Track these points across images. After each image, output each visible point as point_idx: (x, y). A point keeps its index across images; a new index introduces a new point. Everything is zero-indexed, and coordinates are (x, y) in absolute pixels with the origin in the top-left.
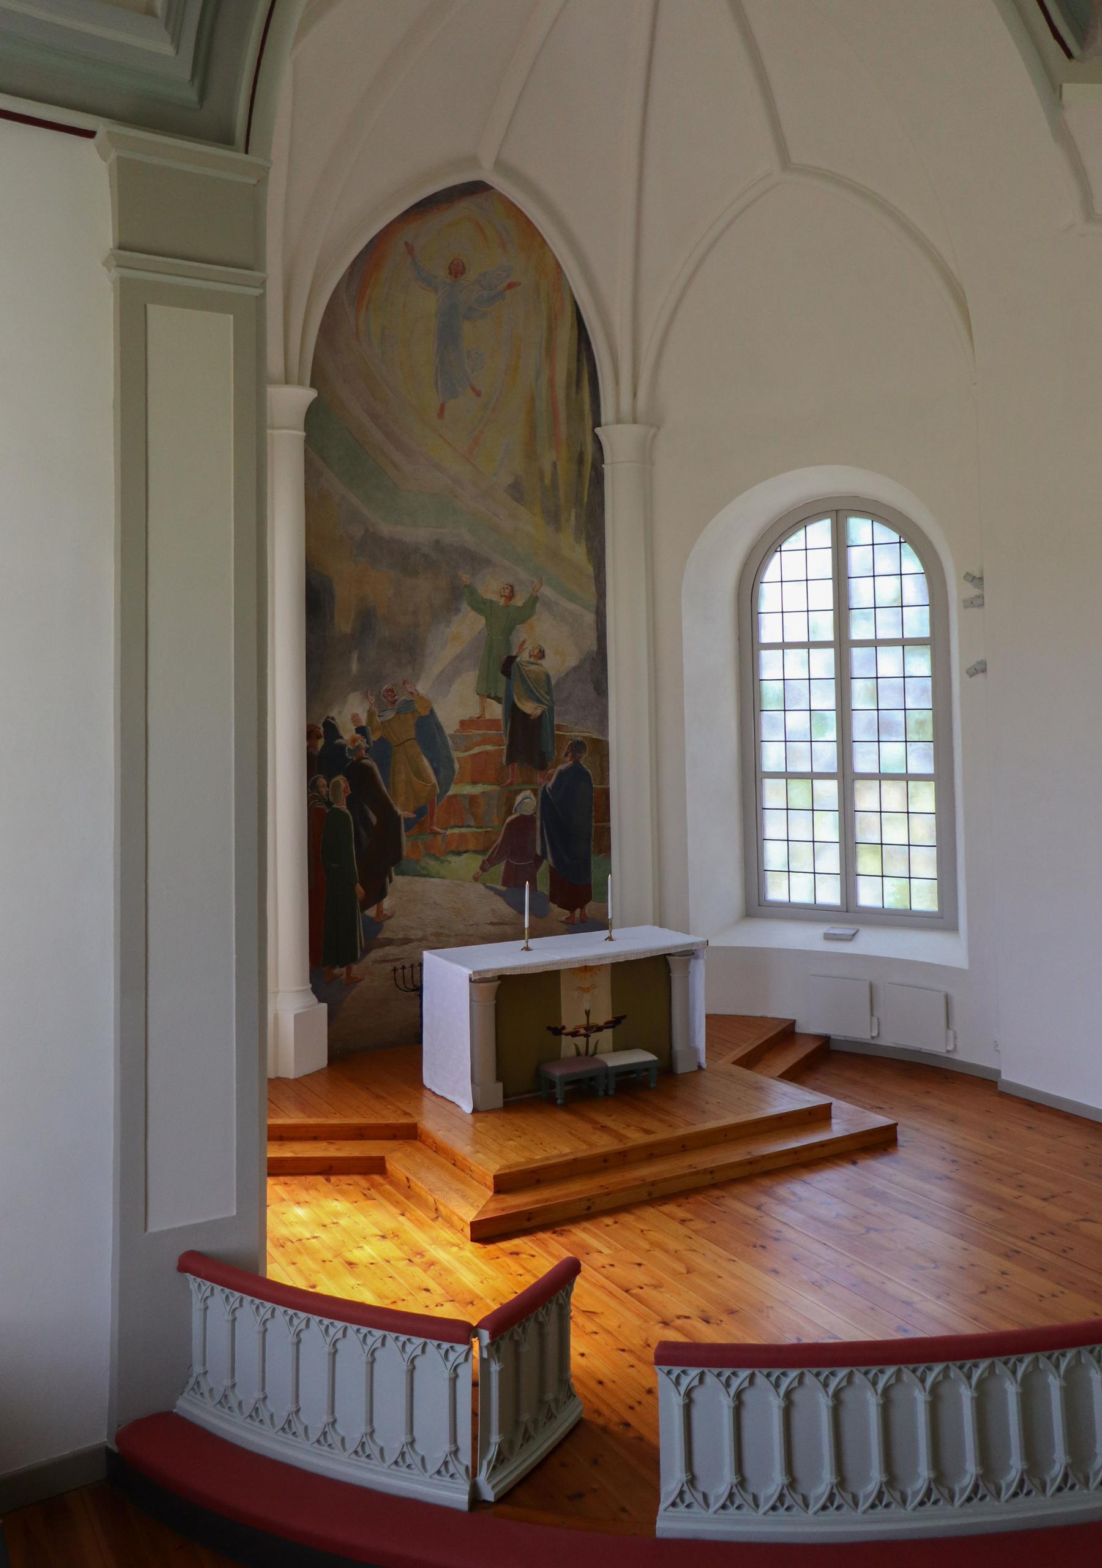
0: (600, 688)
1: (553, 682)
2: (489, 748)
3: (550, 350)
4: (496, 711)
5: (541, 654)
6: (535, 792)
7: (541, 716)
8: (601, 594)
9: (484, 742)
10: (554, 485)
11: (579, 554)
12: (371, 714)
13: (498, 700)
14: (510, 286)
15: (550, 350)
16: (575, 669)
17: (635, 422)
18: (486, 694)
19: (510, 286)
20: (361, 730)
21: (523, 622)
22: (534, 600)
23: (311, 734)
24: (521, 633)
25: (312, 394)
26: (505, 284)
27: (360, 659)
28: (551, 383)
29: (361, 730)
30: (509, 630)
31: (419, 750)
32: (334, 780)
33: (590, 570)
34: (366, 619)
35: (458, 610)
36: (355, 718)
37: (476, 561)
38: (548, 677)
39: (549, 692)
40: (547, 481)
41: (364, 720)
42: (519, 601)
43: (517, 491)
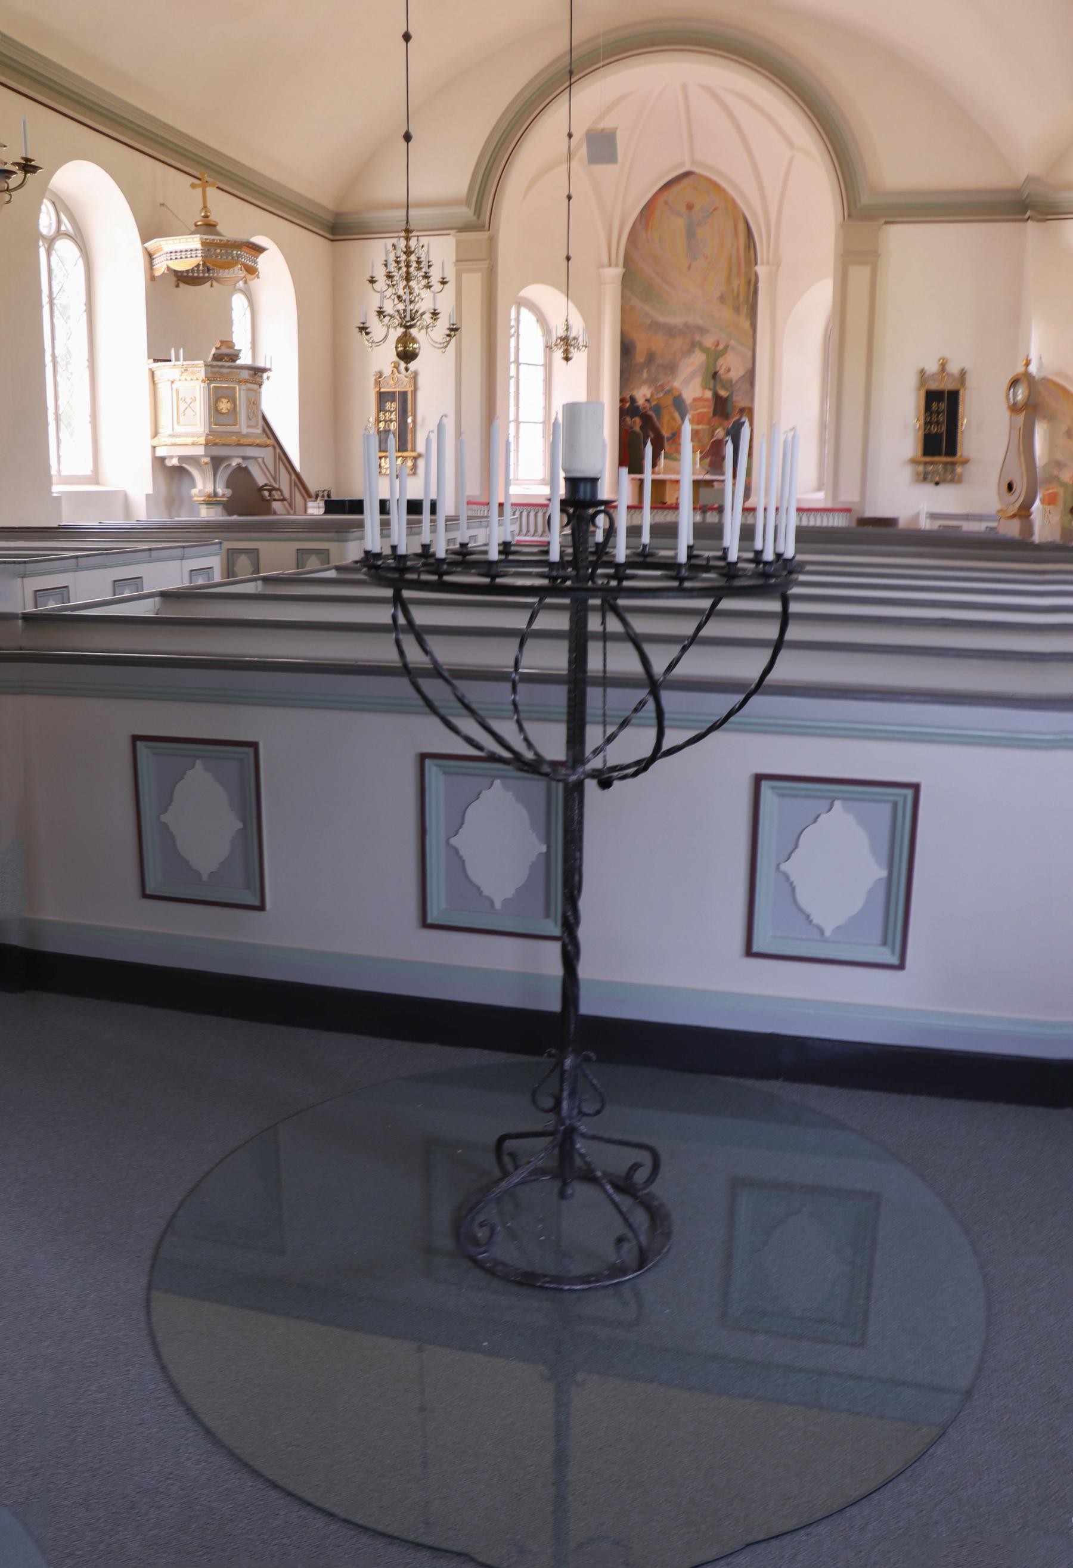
0: (752, 384)
1: (734, 382)
2: (705, 410)
3: (736, 234)
4: (709, 394)
5: (729, 370)
6: (724, 429)
7: (728, 397)
8: (754, 344)
9: (704, 407)
10: (738, 295)
11: (746, 325)
12: (652, 395)
13: (710, 389)
14: (715, 209)
15: (736, 234)
16: (742, 376)
17: (768, 263)
18: (705, 387)
19: (715, 209)
20: (647, 400)
21: (722, 356)
22: (726, 347)
23: (622, 400)
24: (721, 361)
25: (624, 270)
26: (713, 208)
27: (648, 372)
28: (738, 250)
29: (647, 400)
30: (716, 360)
31: (673, 409)
32: (633, 419)
33: (751, 332)
34: (651, 357)
35: (694, 352)
36: (644, 396)
37: (702, 330)
38: (732, 381)
39: (732, 386)
40: (735, 293)
41: (648, 396)
42: (721, 347)
43: (722, 299)
